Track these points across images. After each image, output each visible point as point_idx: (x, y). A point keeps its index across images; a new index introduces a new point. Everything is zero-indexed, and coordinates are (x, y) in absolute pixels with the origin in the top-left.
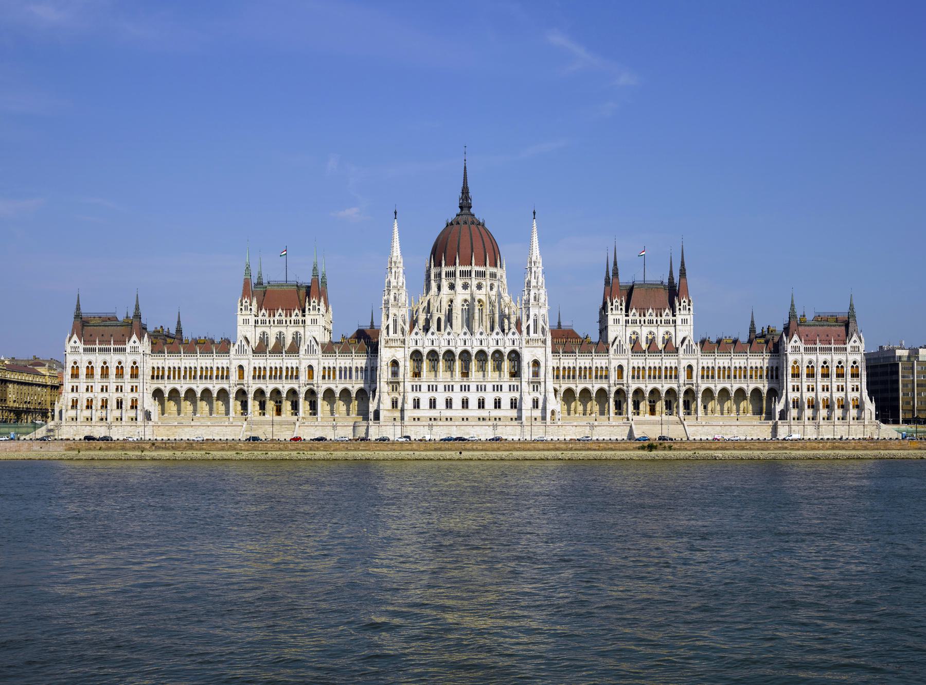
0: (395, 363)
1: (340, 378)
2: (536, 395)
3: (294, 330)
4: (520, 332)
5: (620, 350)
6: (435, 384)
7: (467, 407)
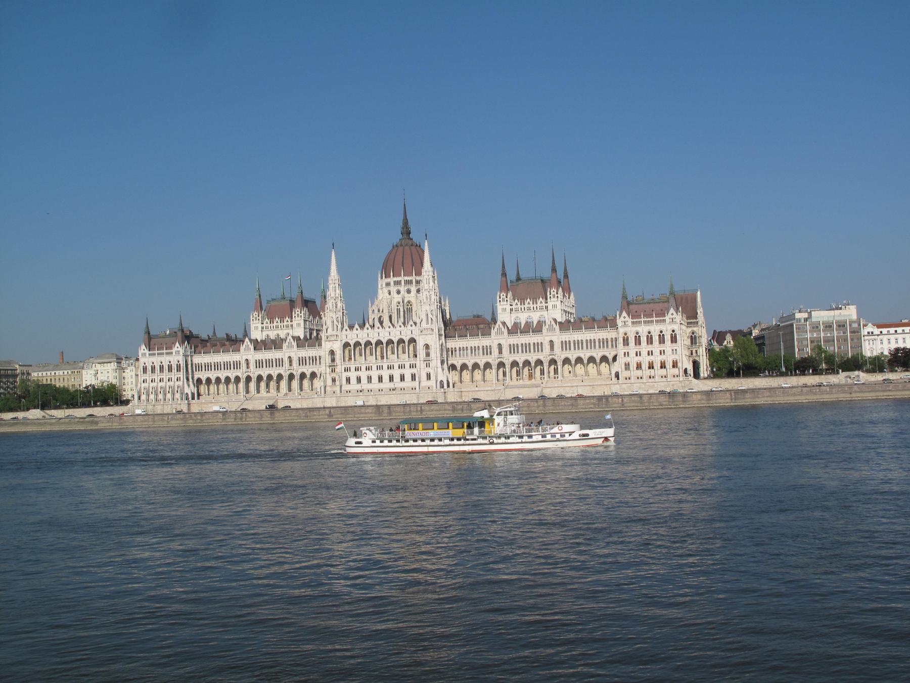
0: (332, 353)
3: (286, 332)
4: (415, 324)
5: (500, 332)
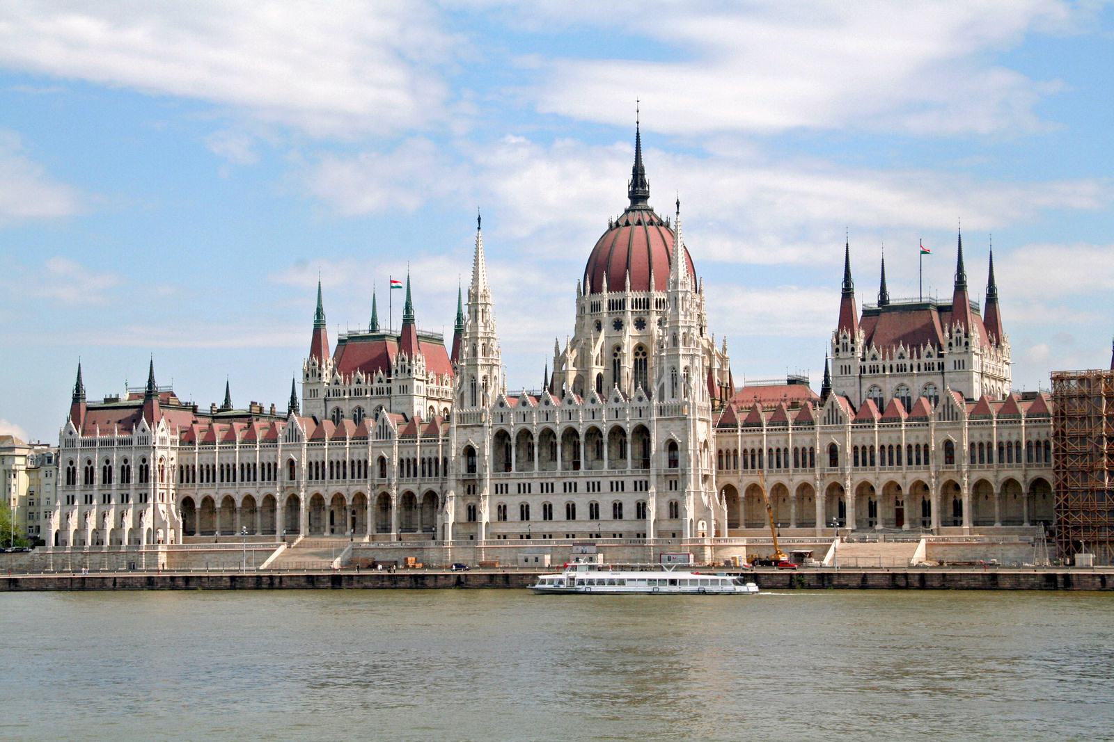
0: (470, 452)
1: (423, 474)
2: (673, 495)
3: (376, 403)
4: (649, 395)
6: (527, 481)
7: (574, 518)
